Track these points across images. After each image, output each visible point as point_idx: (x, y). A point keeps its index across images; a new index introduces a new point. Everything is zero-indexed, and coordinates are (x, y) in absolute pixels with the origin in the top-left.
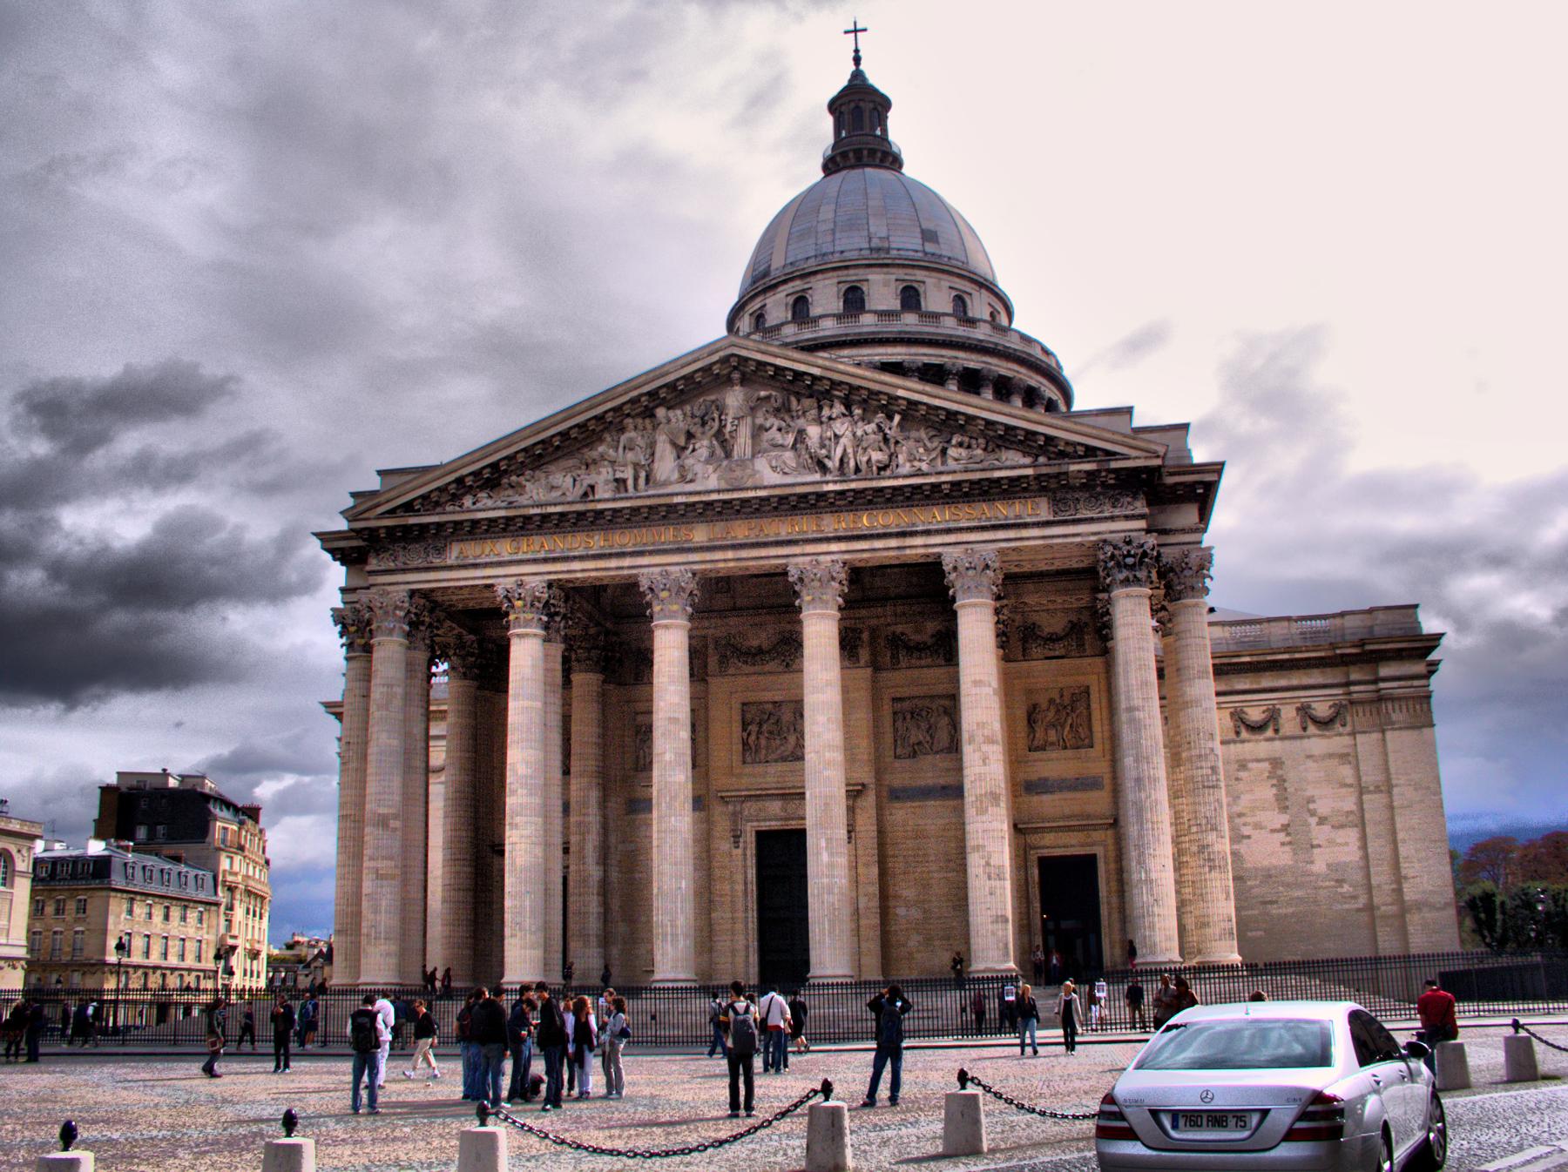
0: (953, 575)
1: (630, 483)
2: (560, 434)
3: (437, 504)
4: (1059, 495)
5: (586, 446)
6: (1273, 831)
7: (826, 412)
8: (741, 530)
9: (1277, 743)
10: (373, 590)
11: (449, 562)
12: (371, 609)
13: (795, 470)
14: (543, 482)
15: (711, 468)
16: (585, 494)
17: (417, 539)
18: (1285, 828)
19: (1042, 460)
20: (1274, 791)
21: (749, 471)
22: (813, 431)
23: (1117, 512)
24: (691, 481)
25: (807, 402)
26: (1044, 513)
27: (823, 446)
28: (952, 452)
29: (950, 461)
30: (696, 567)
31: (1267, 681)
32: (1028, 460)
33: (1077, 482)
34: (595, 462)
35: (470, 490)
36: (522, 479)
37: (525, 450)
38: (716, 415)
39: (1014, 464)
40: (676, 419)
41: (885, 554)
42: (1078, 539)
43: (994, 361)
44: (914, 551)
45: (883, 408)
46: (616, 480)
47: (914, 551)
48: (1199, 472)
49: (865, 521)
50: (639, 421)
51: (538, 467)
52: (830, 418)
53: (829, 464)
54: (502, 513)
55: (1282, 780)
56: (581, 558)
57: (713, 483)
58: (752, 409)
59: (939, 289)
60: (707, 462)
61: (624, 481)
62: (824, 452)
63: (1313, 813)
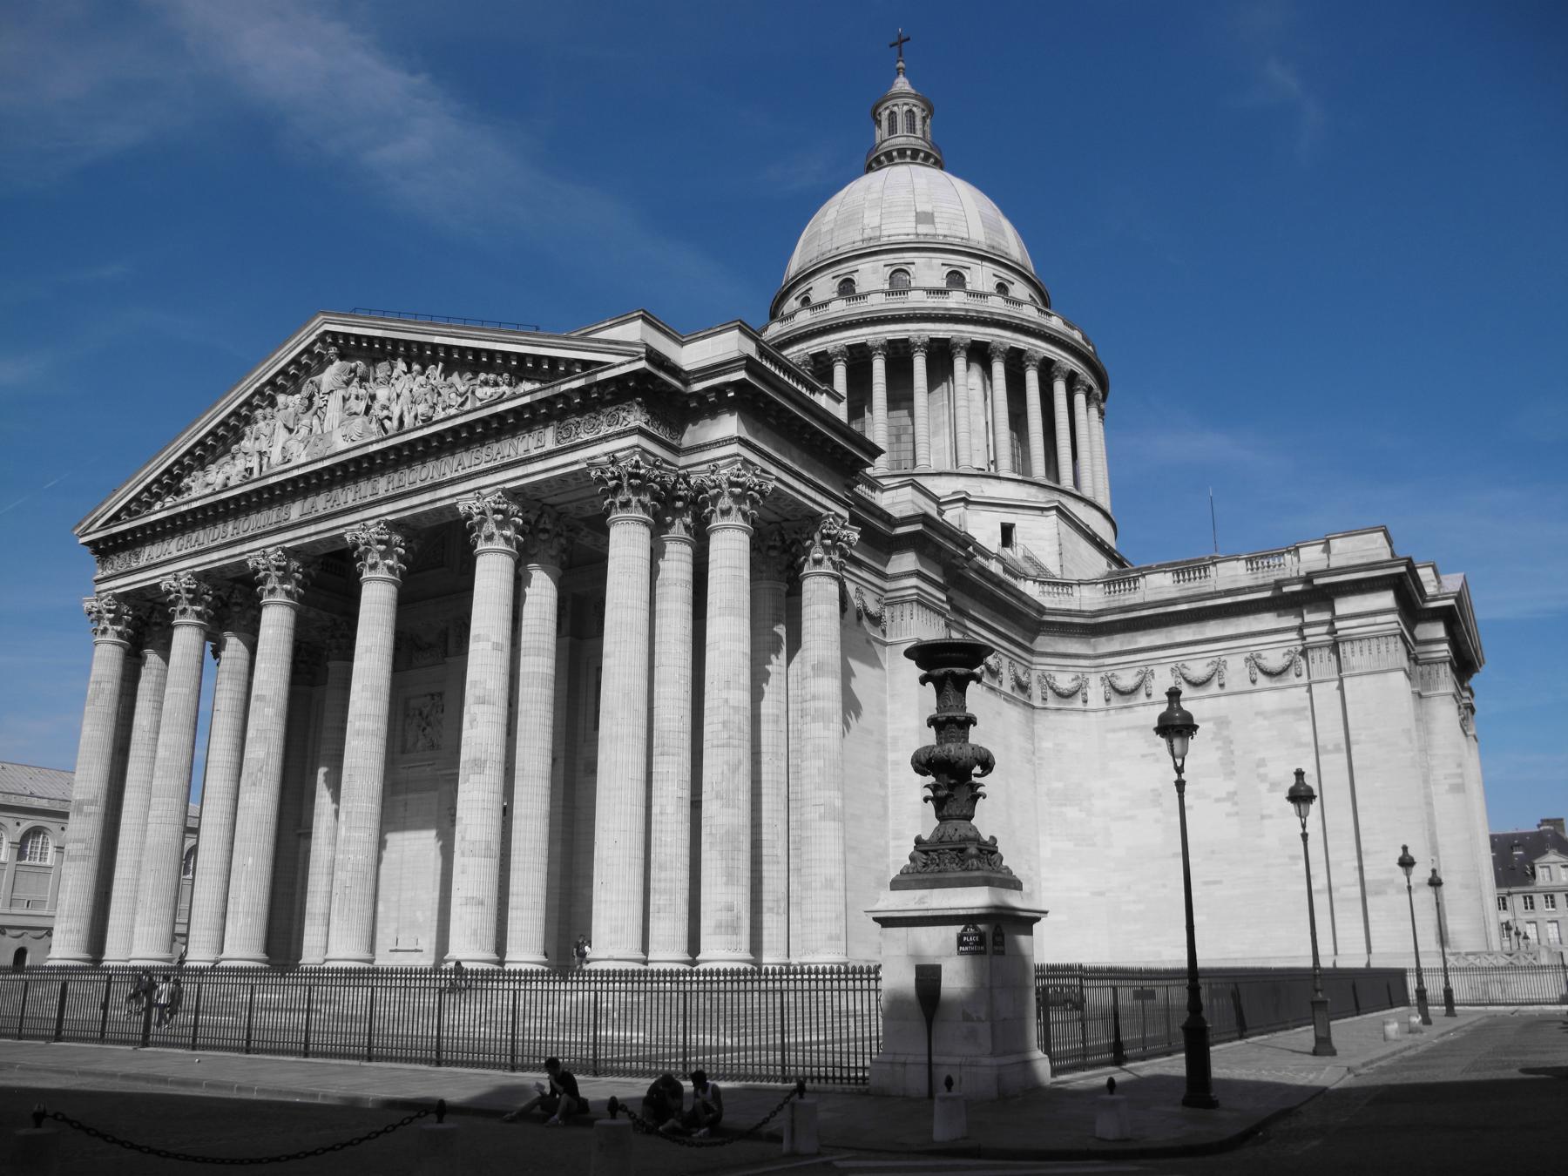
1: (256, 471)
6: (1218, 800)
9: (1223, 699)
18: (1231, 796)
20: (1219, 754)
22: (382, 394)
23: (611, 430)
27: (385, 407)
31: (1213, 629)
35: (158, 497)
39: (528, 391)
43: (970, 328)
48: (725, 373)
53: (387, 423)
55: (1229, 742)
57: (303, 460)
59: (930, 267)
61: (251, 469)
62: (385, 413)
63: (1263, 778)
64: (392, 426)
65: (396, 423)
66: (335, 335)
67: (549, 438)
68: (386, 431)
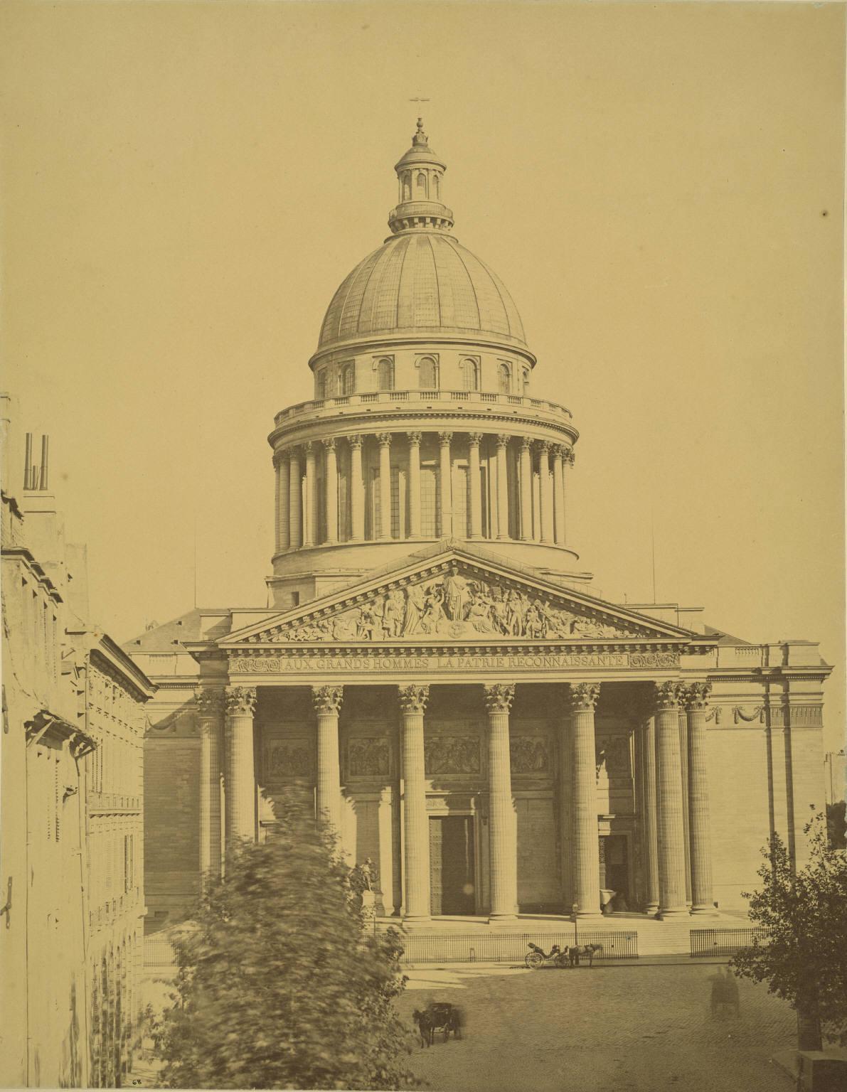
7: (506, 596)
11: (282, 671)
16: (366, 635)
19: (627, 633)
22: (501, 608)
26: (625, 663)
28: (576, 625)
29: (575, 631)
32: (619, 633)
38: (443, 595)
45: (539, 597)
46: (384, 628)
50: (396, 592)
52: (508, 600)
56: (363, 673)
61: (388, 629)
67: (624, 659)
68: (505, 631)
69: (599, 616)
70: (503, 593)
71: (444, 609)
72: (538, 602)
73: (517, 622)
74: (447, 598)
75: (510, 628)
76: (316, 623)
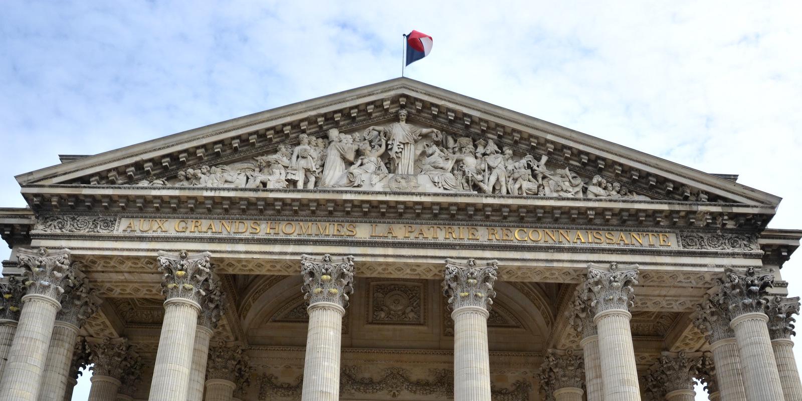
0: (596, 289)
2: (238, 137)
3: (113, 182)
4: (685, 234)
5: (262, 155)
7: (481, 150)
8: (400, 232)
10: (35, 251)
11: (115, 233)
12: (27, 267)
13: (454, 187)
14: (219, 175)
15: (375, 179)
17: (89, 210)
21: (412, 184)
22: (471, 163)
23: (736, 250)
24: (359, 186)
25: (464, 140)
28: (593, 189)
30: (357, 259)
33: (702, 224)
34: (269, 164)
35: (146, 175)
36: (198, 172)
37: (203, 146)
40: (347, 142)
41: (534, 264)
42: (705, 269)
44: (560, 265)
46: (287, 180)
47: (560, 265)
49: (516, 236)
50: (314, 138)
51: (215, 165)
52: (484, 154)
53: (484, 186)
54: (176, 193)
56: (247, 241)
58: (416, 141)
60: (375, 173)
62: (480, 177)
64: (488, 188)
65: (491, 189)
66: (411, 101)
69: (625, 179)
70: (476, 146)
71: (386, 164)
72: (529, 157)
73: (498, 179)
74: (390, 147)
75: (488, 188)
76: (183, 173)
